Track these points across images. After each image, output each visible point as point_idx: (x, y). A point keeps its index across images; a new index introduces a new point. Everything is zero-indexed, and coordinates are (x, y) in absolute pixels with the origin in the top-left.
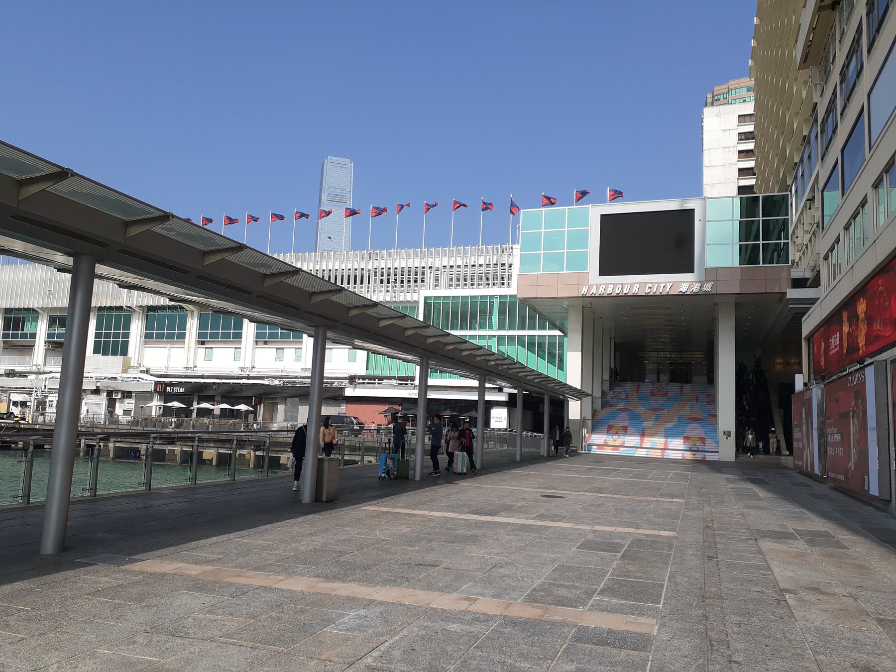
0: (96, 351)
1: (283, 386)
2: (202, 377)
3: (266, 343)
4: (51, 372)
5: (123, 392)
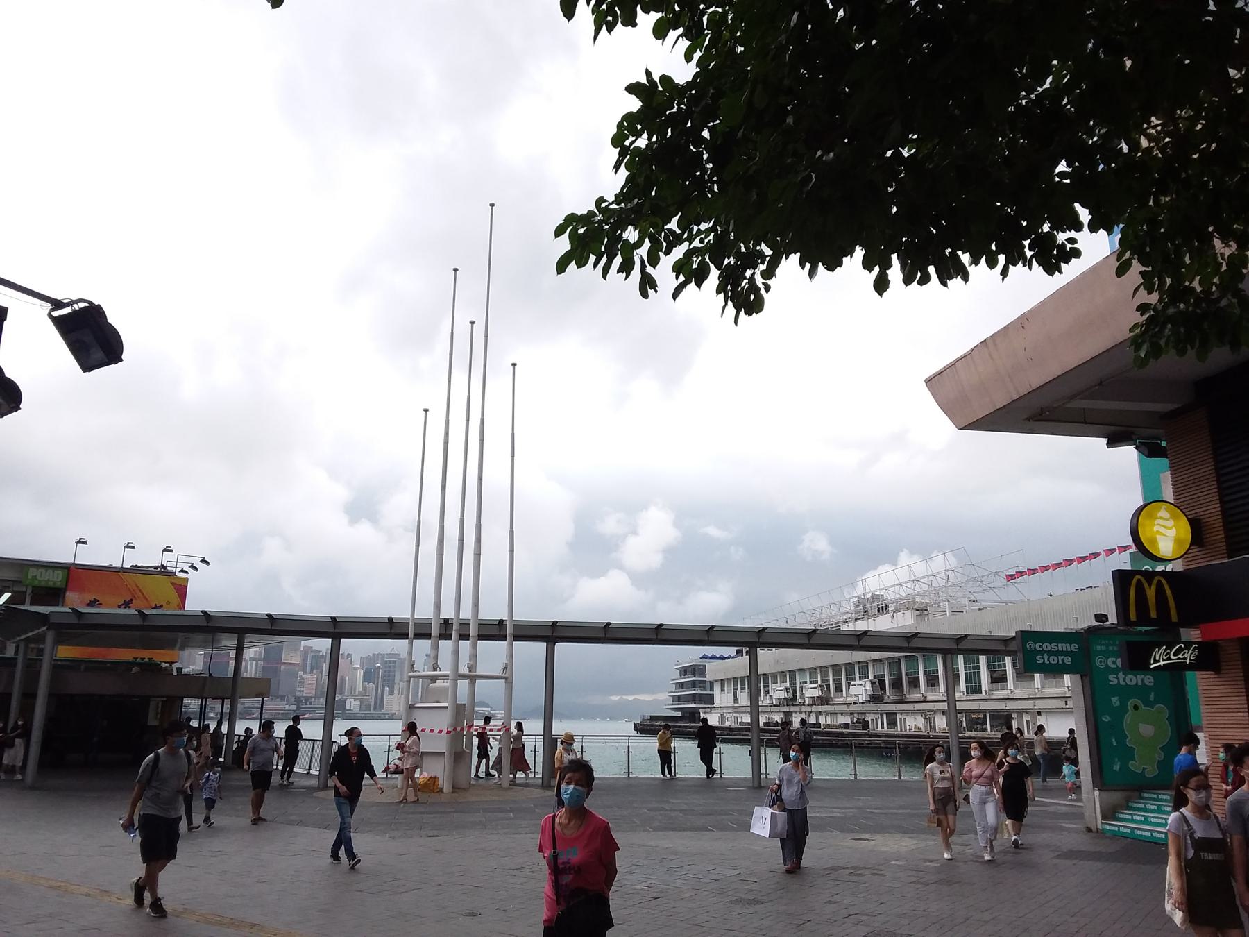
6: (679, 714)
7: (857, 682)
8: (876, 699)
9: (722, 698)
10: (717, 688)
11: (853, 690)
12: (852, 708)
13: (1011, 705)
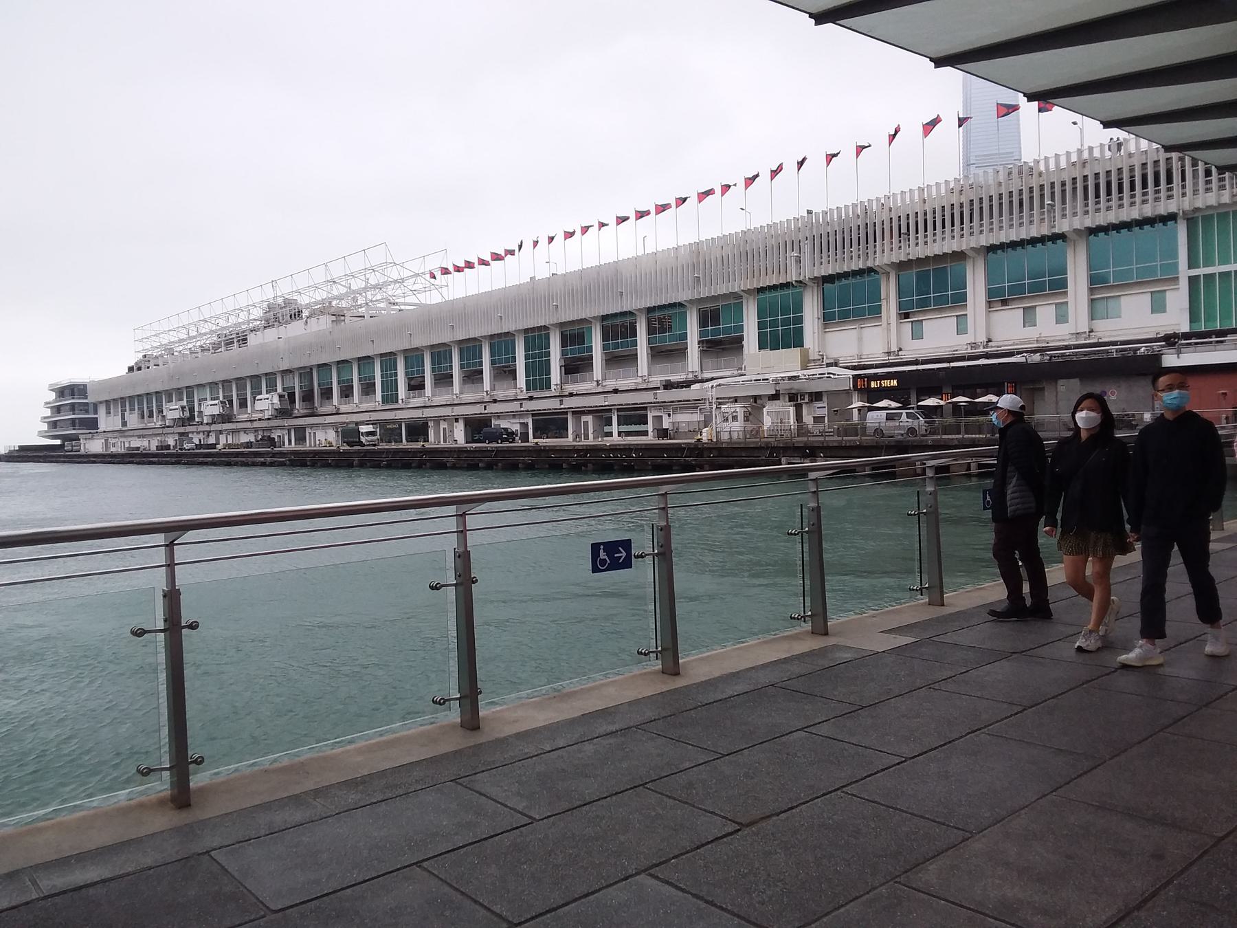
0: (762, 346)
1: (1050, 363)
2: (916, 362)
3: (1004, 303)
4: (712, 379)
5: (810, 394)
6: (58, 442)
7: (264, 396)
8: (283, 413)
9: (107, 422)
10: (102, 411)
11: (259, 405)
12: (256, 425)
13: (428, 413)
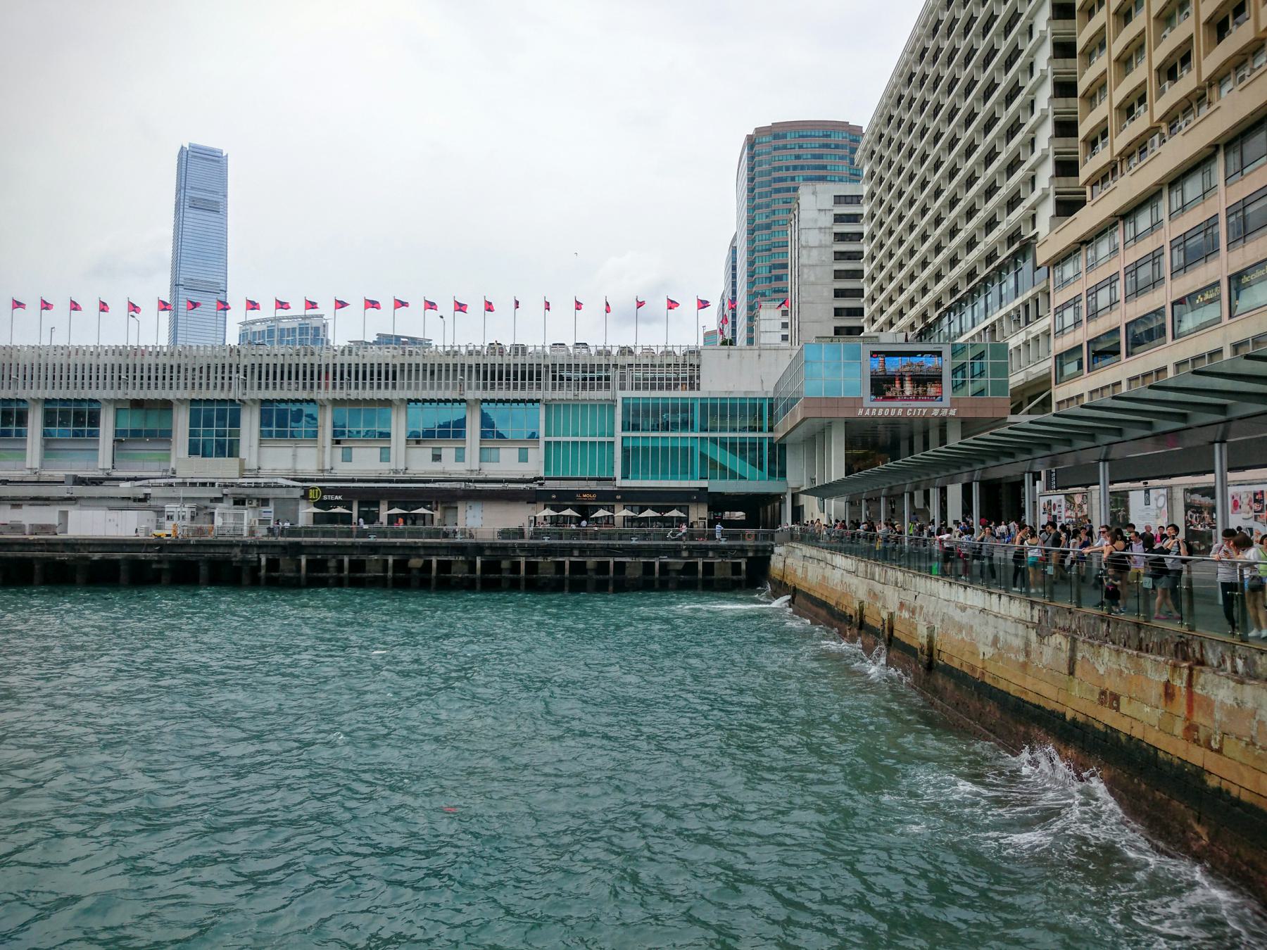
0: (193, 450)
2: (353, 481)
3: (418, 442)
5: (258, 499)
